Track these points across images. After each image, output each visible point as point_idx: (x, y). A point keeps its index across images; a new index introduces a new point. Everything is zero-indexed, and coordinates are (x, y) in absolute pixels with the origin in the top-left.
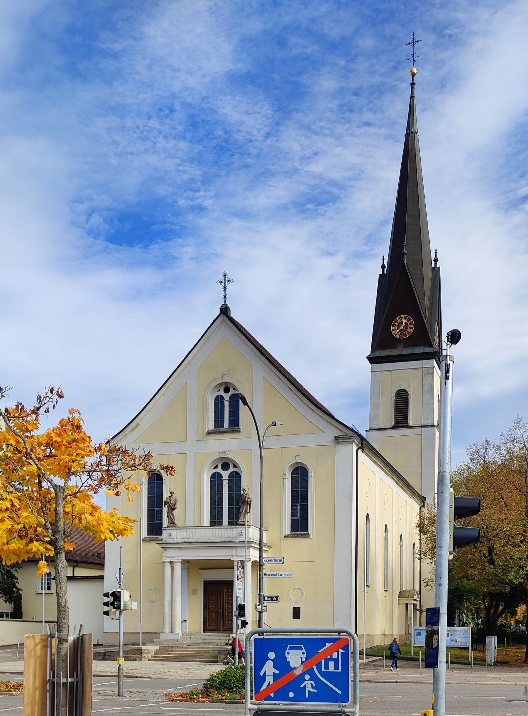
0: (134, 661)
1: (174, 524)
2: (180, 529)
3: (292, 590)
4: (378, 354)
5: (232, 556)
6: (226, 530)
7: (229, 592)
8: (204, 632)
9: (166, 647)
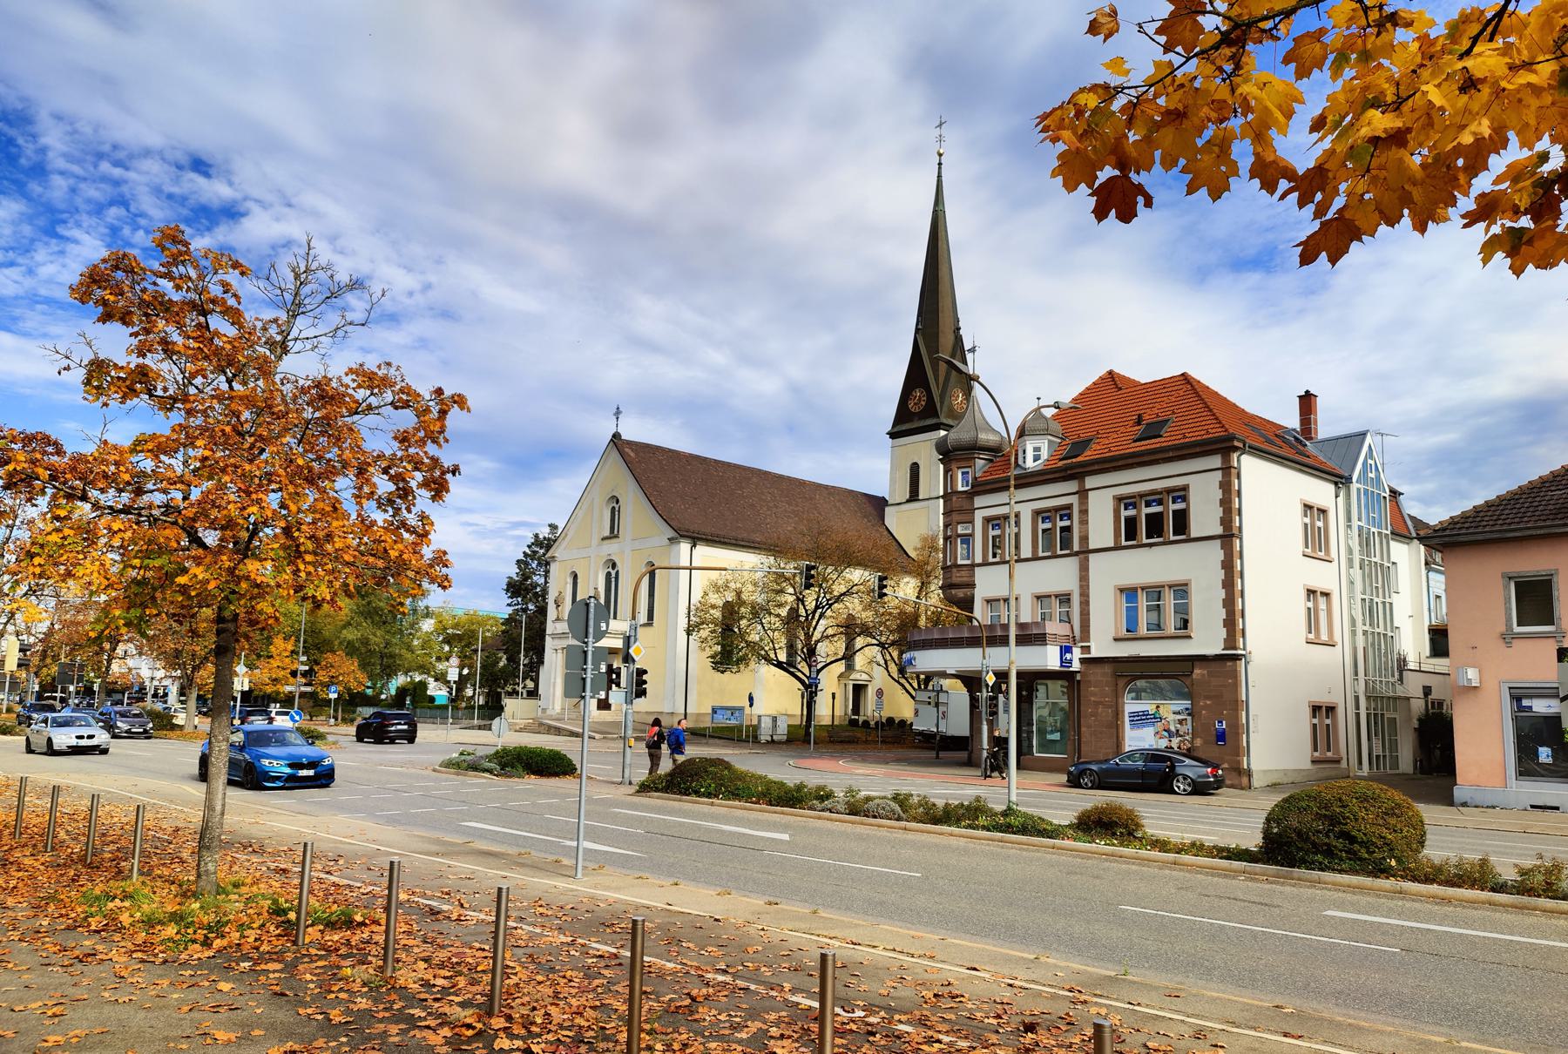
4: (896, 430)
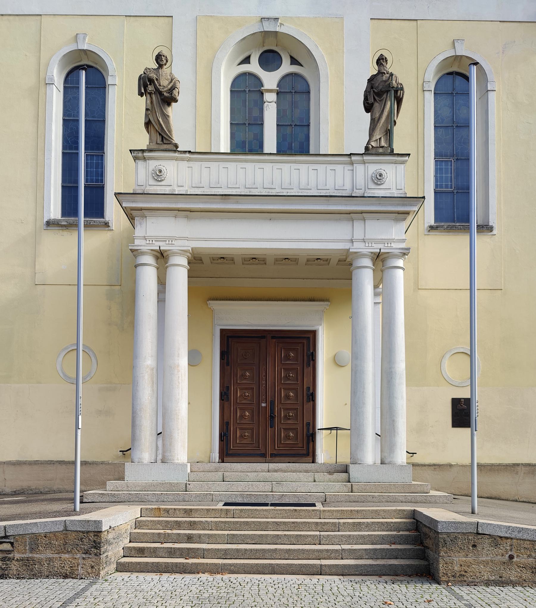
0: (66, 577)
1: (171, 143)
2: (189, 160)
3: (448, 356)
5: (352, 241)
6: (330, 167)
7: (289, 359)
8: (222, 460)
9: (167, 511)
